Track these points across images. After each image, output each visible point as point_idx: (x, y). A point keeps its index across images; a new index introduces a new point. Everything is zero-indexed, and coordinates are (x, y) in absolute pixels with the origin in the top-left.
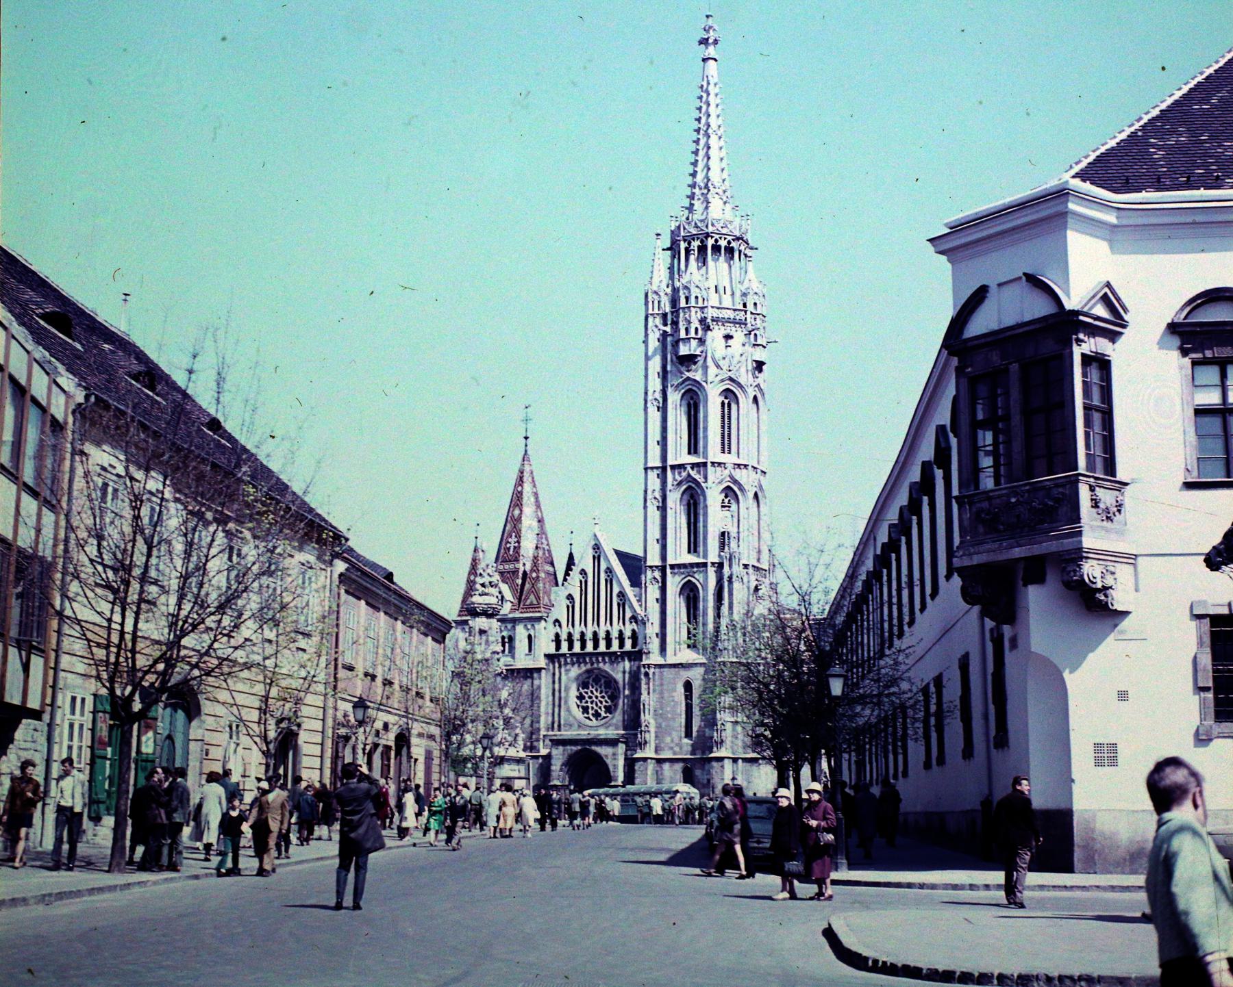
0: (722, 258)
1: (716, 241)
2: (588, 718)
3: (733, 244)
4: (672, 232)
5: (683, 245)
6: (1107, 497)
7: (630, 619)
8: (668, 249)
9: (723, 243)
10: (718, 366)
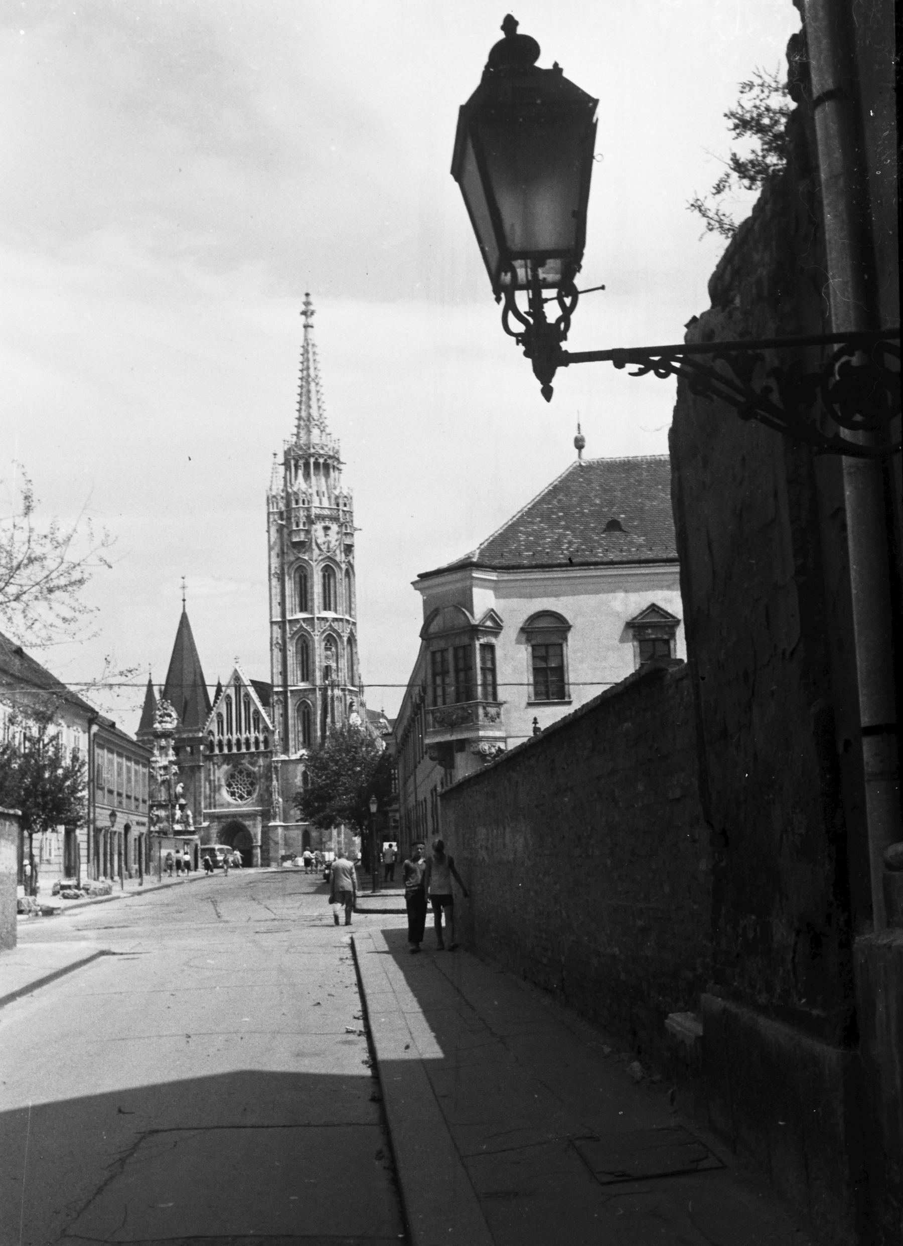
0: (322, 472)
1: (316, 459)
2: (235, 799)
3: (329, 461)
4: (285, 452)
5: (293, 462)
6: (492, 711)
7: (263, 729)
8: (282, 464)
9: (321, 461)
10: (320, 549)
